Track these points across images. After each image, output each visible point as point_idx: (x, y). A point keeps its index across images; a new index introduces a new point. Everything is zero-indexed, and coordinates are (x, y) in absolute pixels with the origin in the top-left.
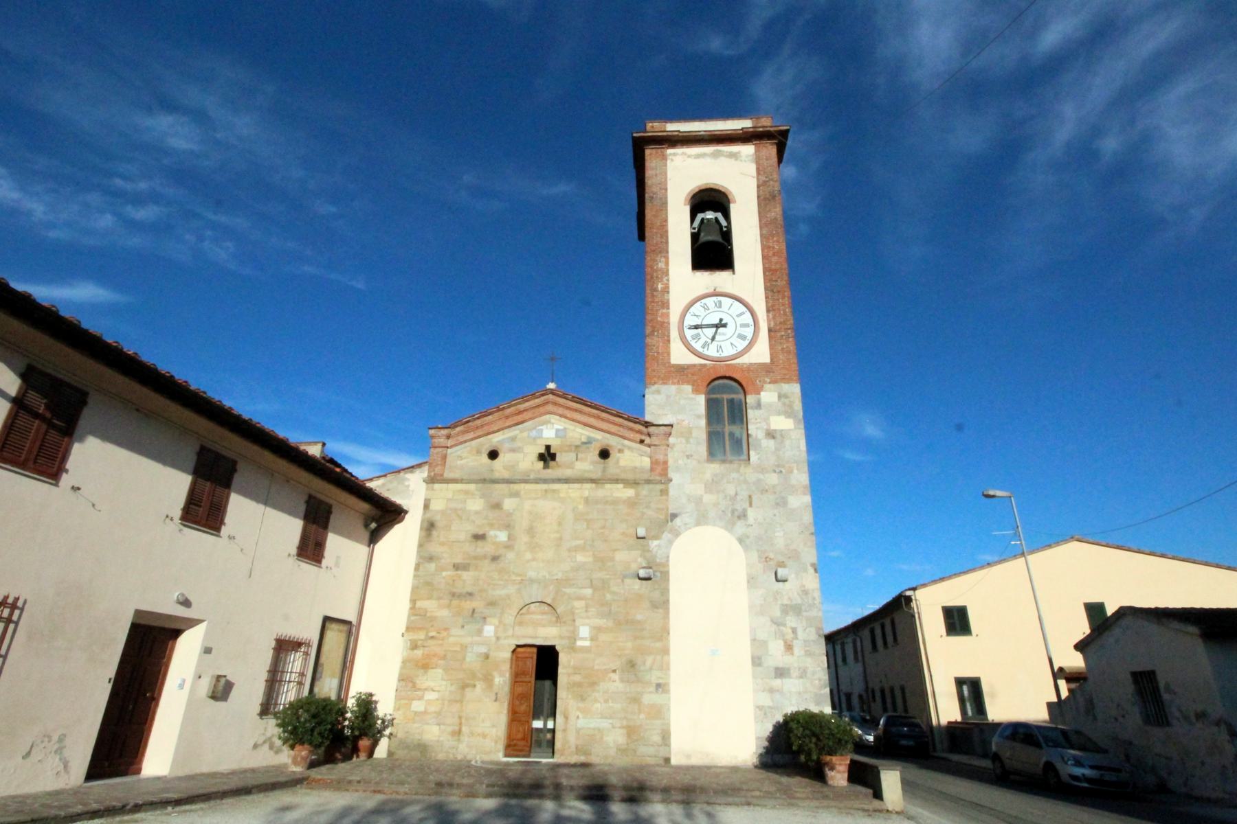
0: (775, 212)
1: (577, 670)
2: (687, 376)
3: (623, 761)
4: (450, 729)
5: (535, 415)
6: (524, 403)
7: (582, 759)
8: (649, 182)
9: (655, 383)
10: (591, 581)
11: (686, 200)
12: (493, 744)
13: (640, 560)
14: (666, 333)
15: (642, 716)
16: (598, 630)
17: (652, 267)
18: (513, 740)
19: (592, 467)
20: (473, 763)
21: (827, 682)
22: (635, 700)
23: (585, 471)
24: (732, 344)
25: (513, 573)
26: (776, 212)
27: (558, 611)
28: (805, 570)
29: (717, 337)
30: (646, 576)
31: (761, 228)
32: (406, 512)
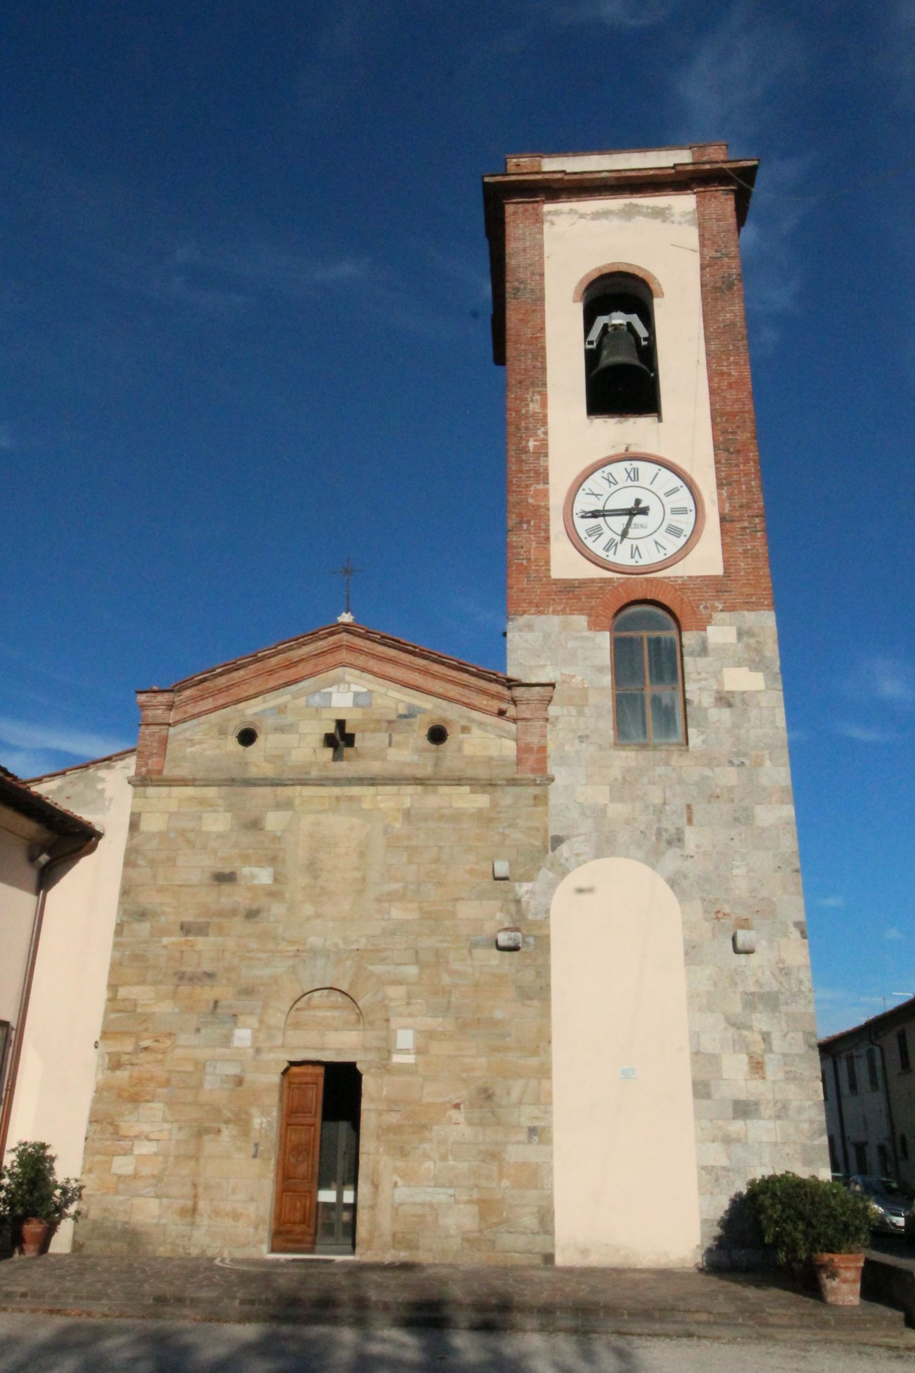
0: (732, 311)
1: (392, 1105)
2: (580, 599)
3: (474, 1259)
4: (179, 1203)
5: (319, 668)
6: (299, 647)
7: (403, 1256)
8: (514, 259)
9: (524, 612)
10: (417, 952)
11: (576, 292)
12: (251, 1230)
13: (499, 916)
14: (543, 526)
15: (505, 1183)
16: (427, 1036)
17: (518, 411)
18: (285, 1223)
19: (416, 758)
20: (217, 1262)
21: (824, 1125)
22: (494, 1155)
23: (410, 764)
24: (656, 543)
25: (283, 939)
27: (360, 1004)
28: (785, 935)
29: (632, 532)
30: (510, 943)
32: (99, 836)
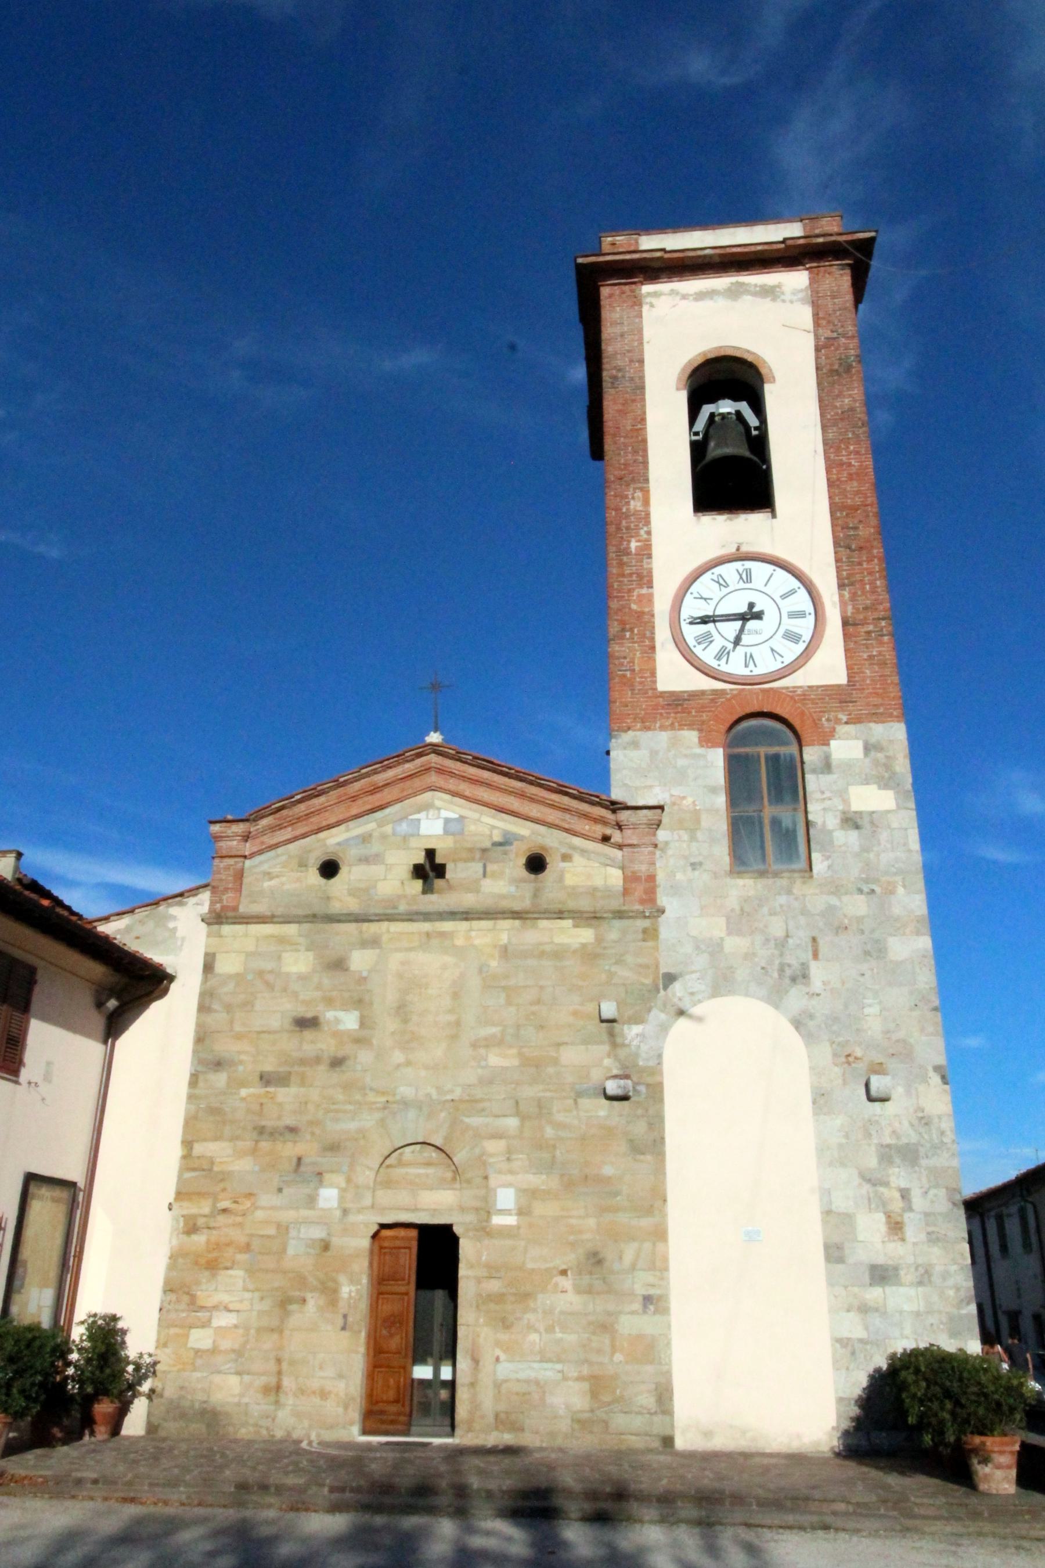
0: (850, 396)
1: (493, 1271)
2: (690, 713)
3: (585, 1443)
4: (262, 1380)
5: (405, 793)
6: (384, 771)
7: (508, 1438)
8: (609, 348)
9: (629, 729)
10: (517, 1103)
11: (679, 379)
12: (341, 1410)
13: (607, 1062)
14: (648, 634)
15: (618, 1357)
16: (529, 1197)
17: (618, 509)
18: (377, 1402)
19: (513, 889)
20: (304, 1445)
21: (972, 1292)
22: (605, 1327)
23: (503, 897)
24: (772, 650)
25: (371, 1089)
26: (853, 395)
27: (455, 1159)
28: (925, 1080)
29: (746, 639)
30: (619, 1092)
31: (824, 428)
32: (171, 978)
